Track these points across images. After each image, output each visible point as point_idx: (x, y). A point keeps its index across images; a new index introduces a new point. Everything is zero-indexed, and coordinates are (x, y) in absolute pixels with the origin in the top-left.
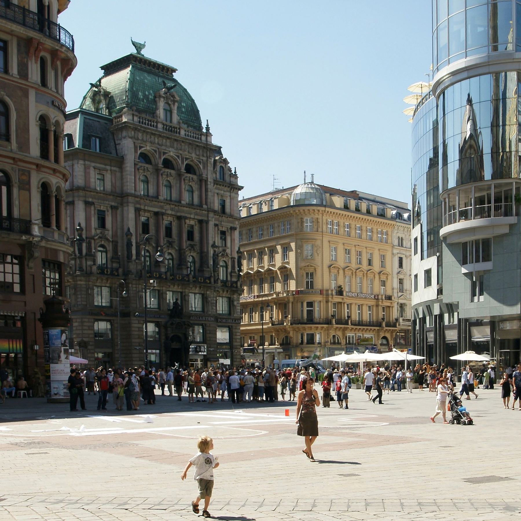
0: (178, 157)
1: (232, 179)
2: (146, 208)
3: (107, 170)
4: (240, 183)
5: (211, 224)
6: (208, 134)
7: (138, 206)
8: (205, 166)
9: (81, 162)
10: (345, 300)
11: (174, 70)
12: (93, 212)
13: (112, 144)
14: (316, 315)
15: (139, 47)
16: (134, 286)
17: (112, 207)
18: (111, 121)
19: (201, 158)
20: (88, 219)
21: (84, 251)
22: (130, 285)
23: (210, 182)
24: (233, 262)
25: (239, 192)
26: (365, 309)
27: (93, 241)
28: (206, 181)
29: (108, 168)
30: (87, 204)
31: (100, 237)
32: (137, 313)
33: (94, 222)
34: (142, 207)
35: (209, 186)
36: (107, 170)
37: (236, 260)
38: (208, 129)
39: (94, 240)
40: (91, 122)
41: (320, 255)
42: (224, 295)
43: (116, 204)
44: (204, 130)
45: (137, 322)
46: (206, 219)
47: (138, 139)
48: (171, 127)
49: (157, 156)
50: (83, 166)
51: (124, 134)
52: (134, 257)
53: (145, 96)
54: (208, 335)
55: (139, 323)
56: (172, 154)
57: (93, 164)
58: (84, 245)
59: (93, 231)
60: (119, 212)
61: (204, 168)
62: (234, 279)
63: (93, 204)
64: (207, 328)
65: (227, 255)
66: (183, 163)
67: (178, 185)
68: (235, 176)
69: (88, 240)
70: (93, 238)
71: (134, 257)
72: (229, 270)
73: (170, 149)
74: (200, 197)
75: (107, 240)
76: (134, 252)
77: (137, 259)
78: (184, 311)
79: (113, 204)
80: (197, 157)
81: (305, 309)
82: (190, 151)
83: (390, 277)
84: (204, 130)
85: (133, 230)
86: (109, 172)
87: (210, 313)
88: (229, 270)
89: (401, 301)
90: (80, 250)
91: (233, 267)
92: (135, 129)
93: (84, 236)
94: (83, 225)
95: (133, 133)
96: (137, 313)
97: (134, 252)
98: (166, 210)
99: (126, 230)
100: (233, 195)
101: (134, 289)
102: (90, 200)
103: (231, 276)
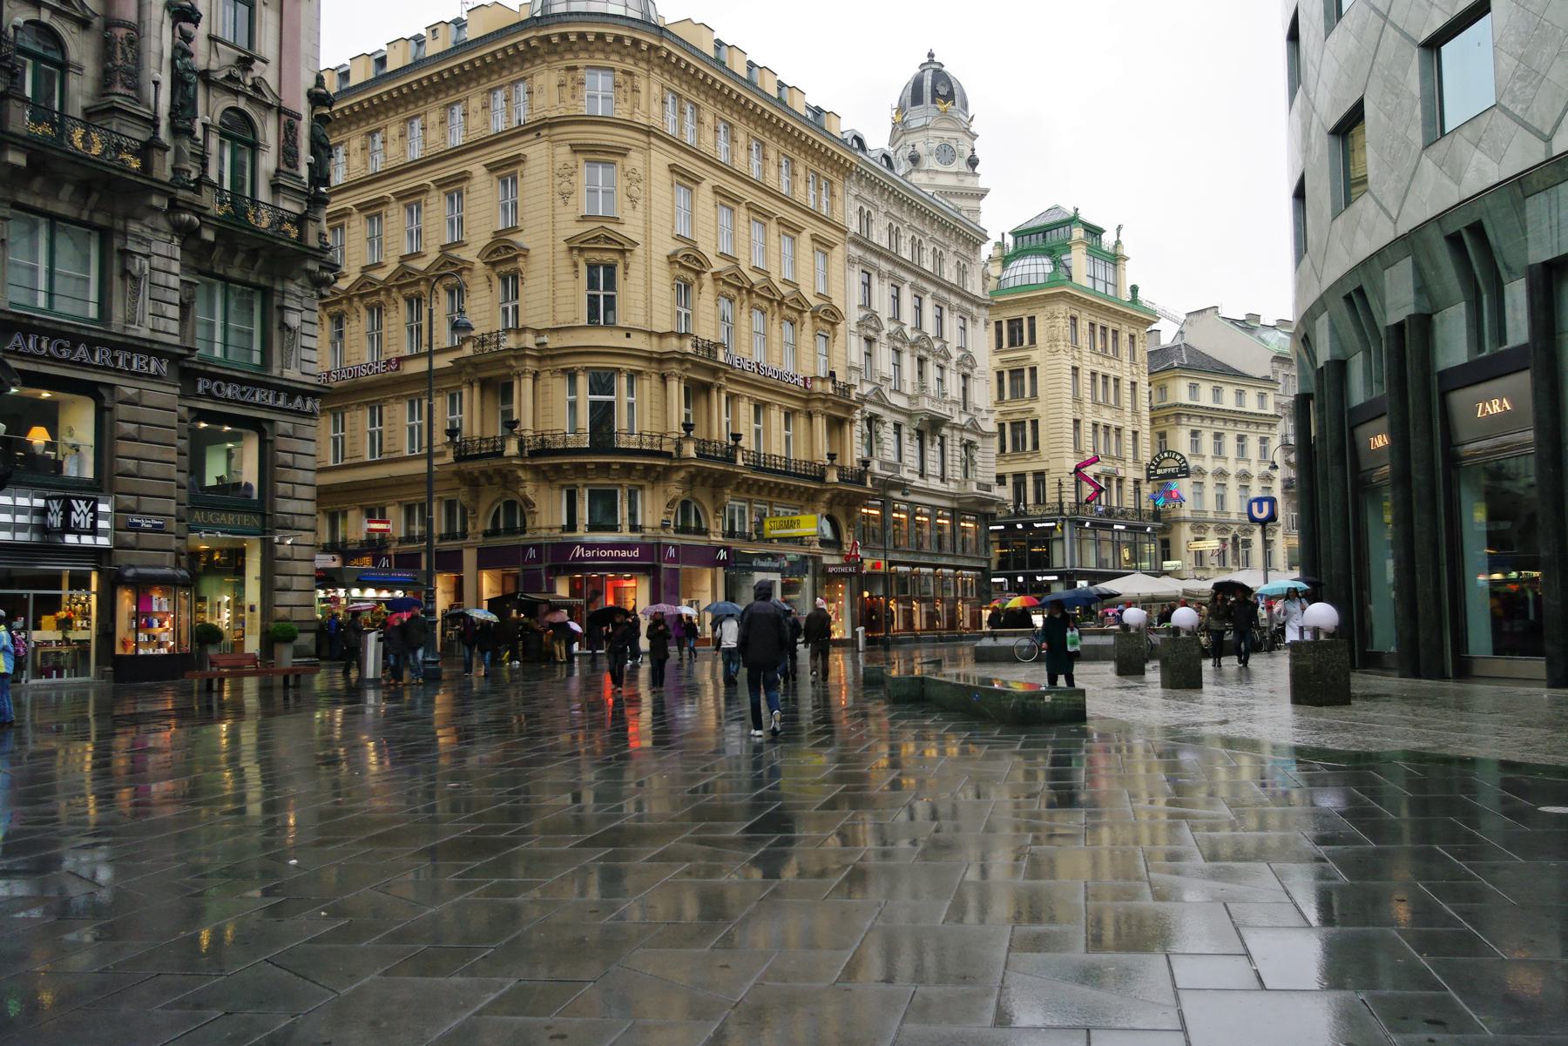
10: (723, 382)
14: (621, 421)
26: (776, 417)
37: (304, 128)
41: (640, 207)
42: (235, 273)
54: (124, 448)
62: (290, 206)
64: (123, 410)
65: (255, 87)
72: (268, 161)
81: (584, 398)
83: (840, 327)
88: (268, 161)
89: (869, 408)
91: (288, 153)
103: (276, 188)
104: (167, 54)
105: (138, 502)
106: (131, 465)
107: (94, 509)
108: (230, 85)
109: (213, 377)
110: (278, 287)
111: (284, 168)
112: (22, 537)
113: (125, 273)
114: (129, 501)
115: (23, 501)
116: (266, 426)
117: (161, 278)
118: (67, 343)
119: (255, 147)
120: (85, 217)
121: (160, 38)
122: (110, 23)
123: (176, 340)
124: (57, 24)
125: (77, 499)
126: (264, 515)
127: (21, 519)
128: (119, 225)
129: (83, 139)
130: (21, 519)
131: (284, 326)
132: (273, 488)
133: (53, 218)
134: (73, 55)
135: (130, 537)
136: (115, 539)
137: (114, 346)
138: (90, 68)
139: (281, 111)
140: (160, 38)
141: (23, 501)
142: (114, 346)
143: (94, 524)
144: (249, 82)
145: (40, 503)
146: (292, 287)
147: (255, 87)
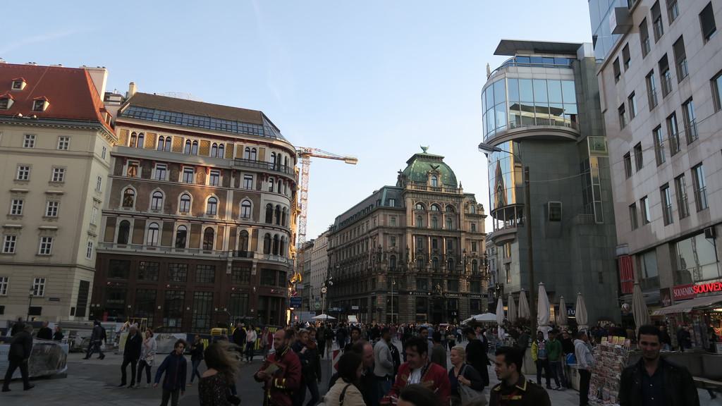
5: (463, 239)
6: (461, 188)
8: (459, 207)
9: (382, 213)
11: (443, 158)
12: (388, 238)
13: (402, 202)
15: (424, 149)
17: (399, 235)
18: (402, 189)
20: (385, 242)
21: (382, 259)
24: (482, 260)
25: (486, 219)
28: (459, 215)
30: (385, 234)
33: (389, 243)
35: (461, 218)
38: (461, 186)
44: (458, 187)
51: (407, 196)
53: (420, 174)
58: (382, 256)
59: (388, 248)
62: (481, 271)
63: (387, 234)
71: (410, 261)
74: (456, 224)
75: (395, 252)
84: (458, 187)
85: (410, 247)
90: (380, 260)
92: (412, 193)
93: (382, 252)
94: (382, 246)
108: (473, 257)
119: (476, 263)
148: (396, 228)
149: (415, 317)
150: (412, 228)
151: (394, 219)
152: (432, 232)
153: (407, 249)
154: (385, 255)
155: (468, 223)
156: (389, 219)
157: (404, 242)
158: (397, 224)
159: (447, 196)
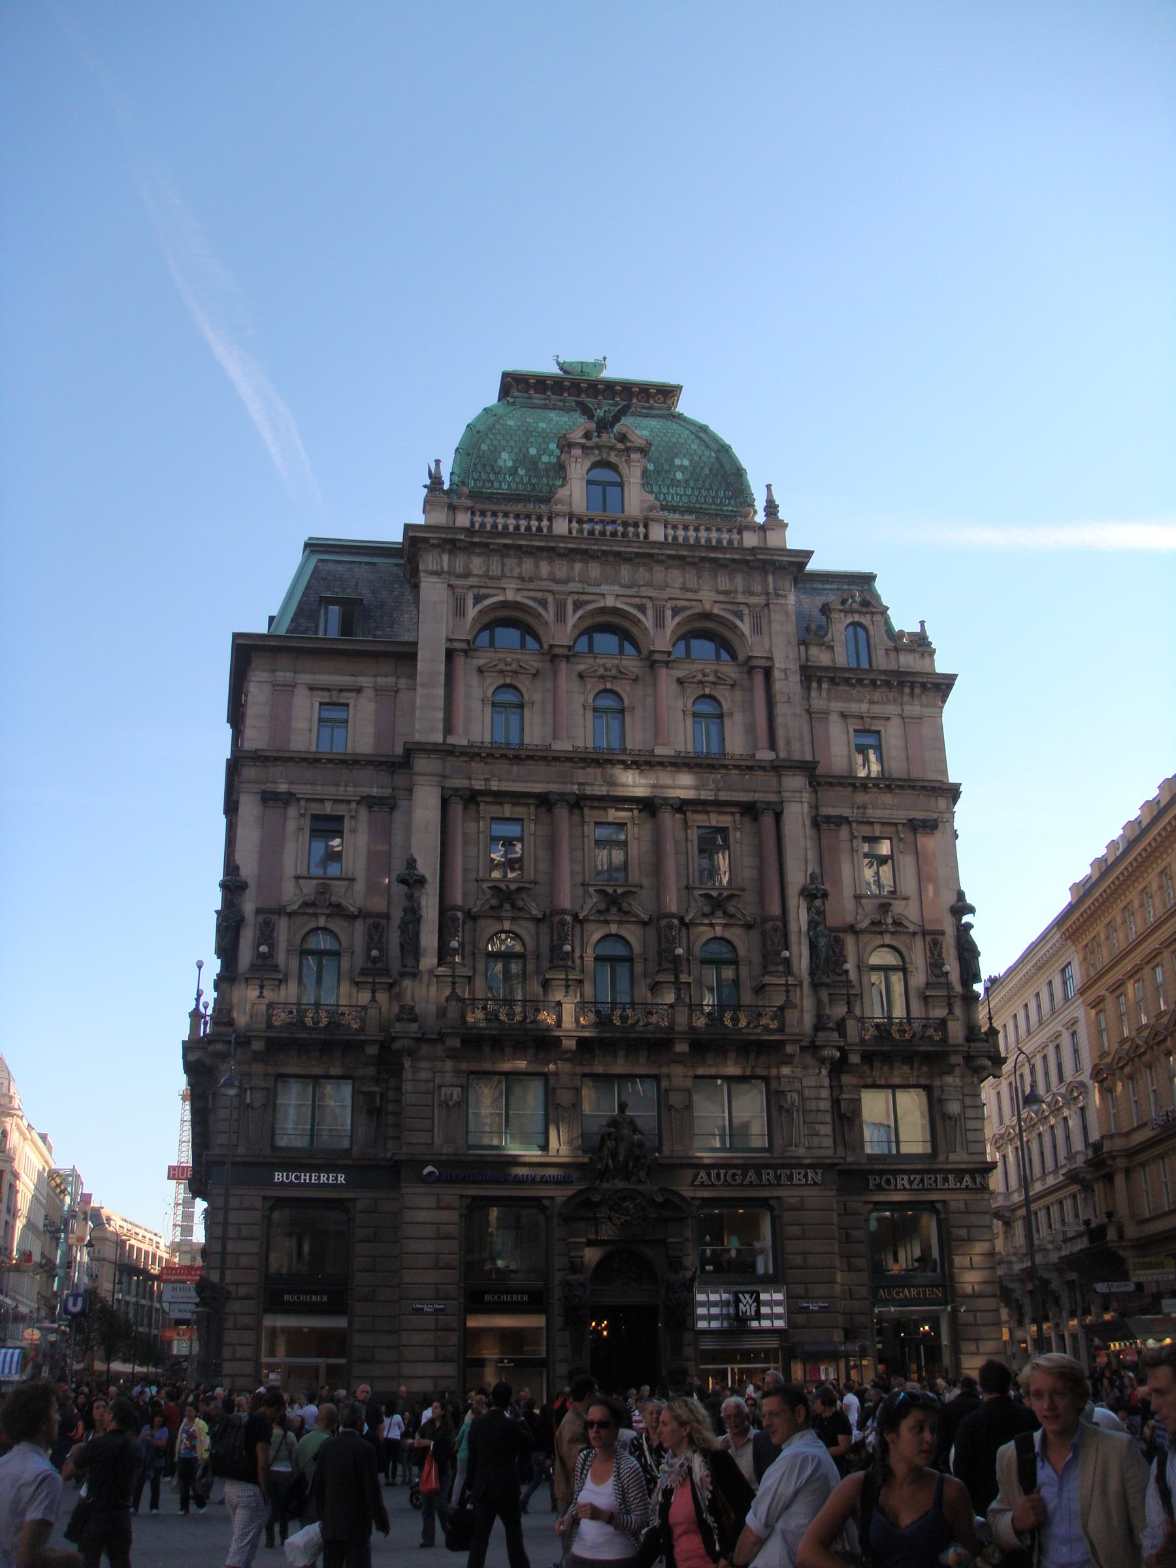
0: (642, 608)
1: (908, 661)
2: (494, 786)
3: (359, 690)
4: (941, 666)
5: (796, 815)
7: (460, 783)
12: (291, 825)
16: (424, 1064)
17: (369, 802)
19: (740, 598)
22: (407, 1063)
23: (785, 671)
27: (283, 925)
28: (768, 672)
29: (364, 681)
31: (306, 904)
32: (429, 1169)
34: (479, 785)
35: (778, 686)
36: (359, 690)
38: (771, 508)
39: (290, 915)
40: (340, 568)
43: (387, 792)
45: (430, 1202)
46: (772, 798)
47: (467, 575)
48: (625, 524)
49: (549, 615)
50: (267, 688)
52: (429, 961)
54: (790, 1246)
55: (438, 1208)
56: (610, 602)
57: (306, 678)
60: (398, 816)
61: (757, 629)
63: (289, 798)
64: (788, 1216)
66: (660, 622)
67: (649, 701)
68: (920, 644)
69: (261, 918)
70: (280, 911)
73: (604, 588)
76: (429, 939)
77: (439, 964)
78: (666, 1149)
79: (374, 791)
80: (721, 598)
82: (692, 583)
84: (760, 518)
85: (427, 866)
86: (369, 693)
87: (801, 1151)
95: (446, 558)
96: (429, 1169)
97: (429, 939)
98: (580, 784)
99: (399, 867)
100: (914, 709)
101: (423, 1075)
102: (283, 788)
104: (804, 928)
105: (807, 1289)
106: (798, 1260)
107: (757, 1300)
109: (881, 1173)
110: (937, 1083)
111: (934, 979)
112: (715, 1324)
113: (781, 1108)
114: (800, 1289)
115: (714, 1297)
116: (939, 1206)
117: (812, 1105)
118: (739, 1172)
120: (748, 1073)
121: (800, 916)
122: (765, 920)
123: (830, 1152)
124: (728, 934)
125: (743, 1293)
126: (944, 1287)
127: (715, 1311)
128: (774, 1072)
129: (732, 1019)
130: (715, 1311)
131: (946, 1117)
132: (951, 1262)
133: (728, 1079)
134: (742, 951)
135: (801, 1319)
136: (789, 1322)
137: (775, 1167)
138: (756, 957)
139: (924, 933)
140: (800, 916)
141: (714, 1297)
142: (775, 1167)
143: (758, 1311)
144: (890, 921)
145: (725, 1296)
146: (949, 1079)
147: (896, 923)
148: (352, 762)
149: (454, 1338)
150: (446, 752)
151: (334, 706)
152: (581, 775)
153: (412, 881)
154: (266, 934)
155: (834, 721)
156: (304, 711)
157: (398, 838)
158: (361, 736)
159: (682, 562)
